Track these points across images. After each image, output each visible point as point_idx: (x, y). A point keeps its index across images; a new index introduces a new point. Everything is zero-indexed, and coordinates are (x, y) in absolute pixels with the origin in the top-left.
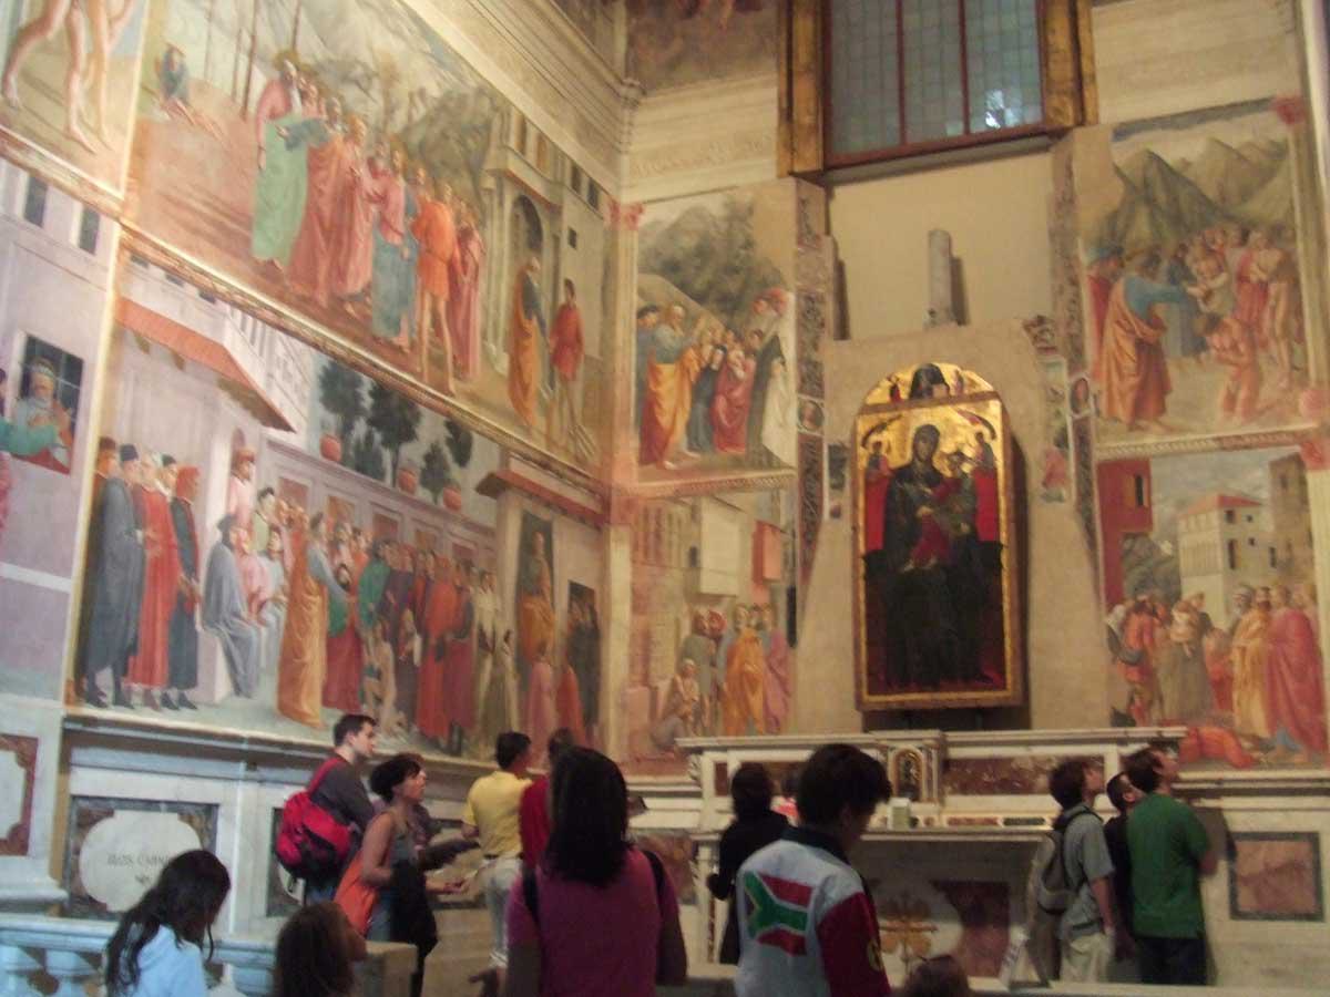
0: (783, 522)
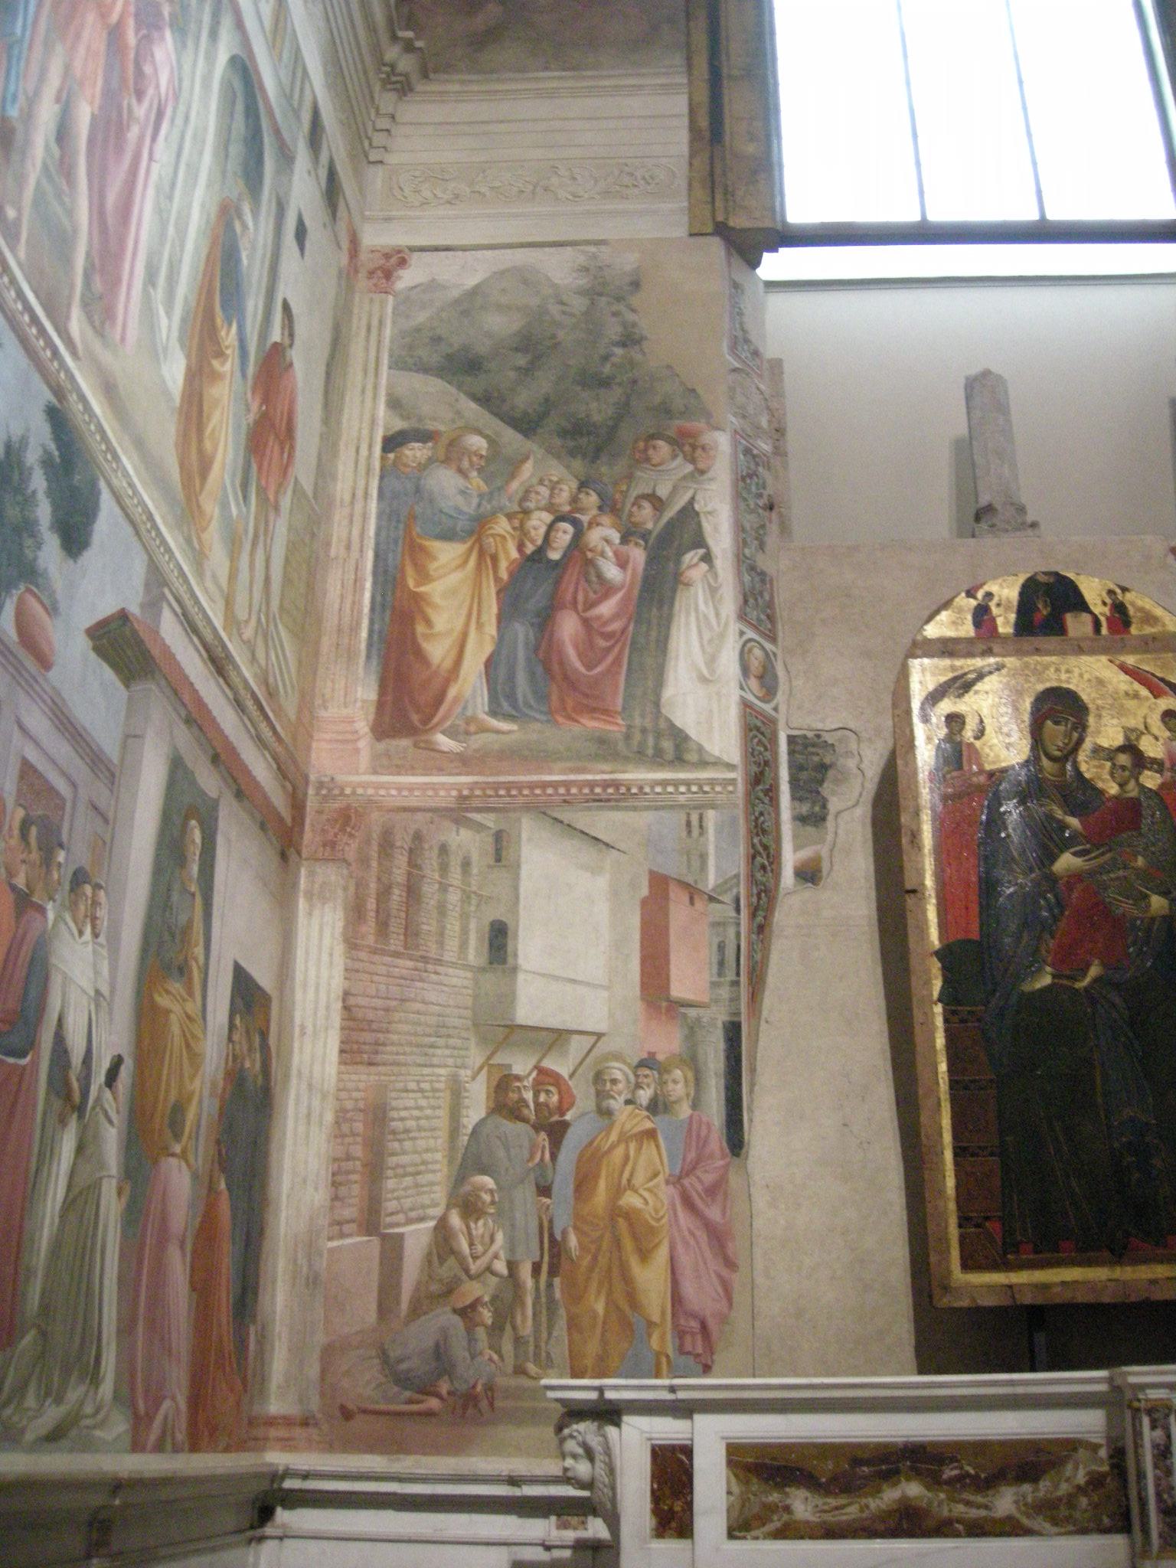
0: (712, 880)
